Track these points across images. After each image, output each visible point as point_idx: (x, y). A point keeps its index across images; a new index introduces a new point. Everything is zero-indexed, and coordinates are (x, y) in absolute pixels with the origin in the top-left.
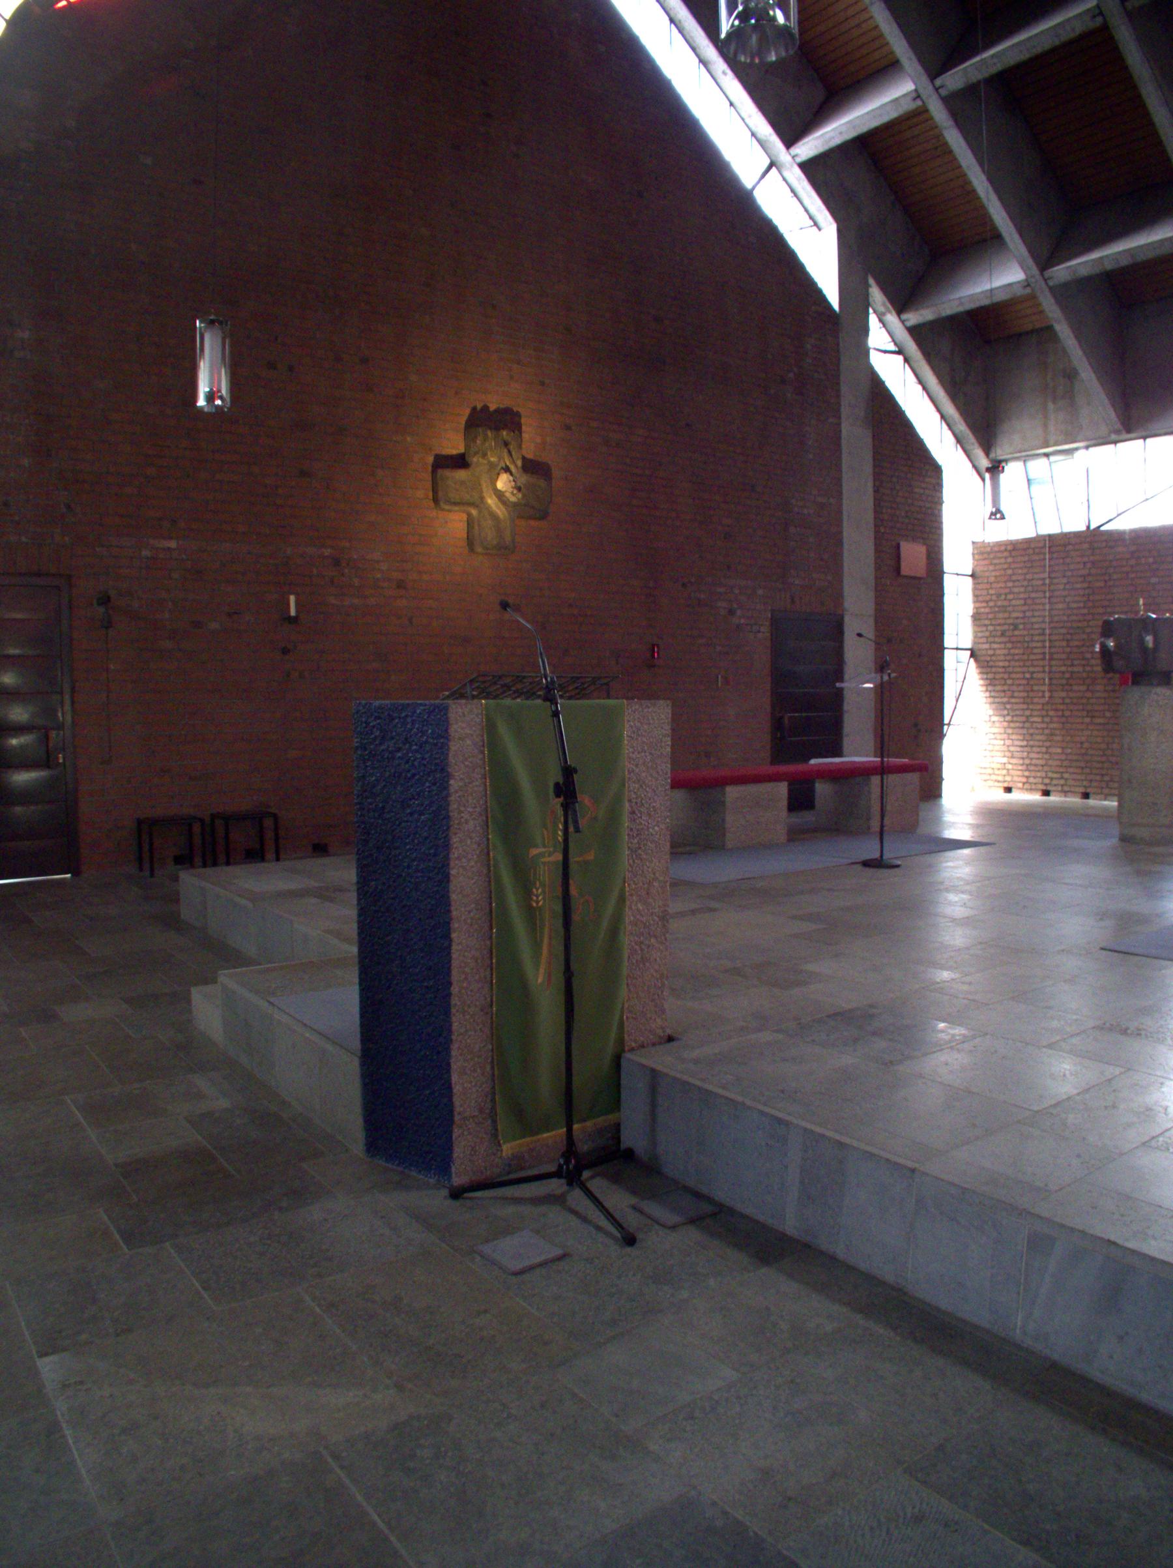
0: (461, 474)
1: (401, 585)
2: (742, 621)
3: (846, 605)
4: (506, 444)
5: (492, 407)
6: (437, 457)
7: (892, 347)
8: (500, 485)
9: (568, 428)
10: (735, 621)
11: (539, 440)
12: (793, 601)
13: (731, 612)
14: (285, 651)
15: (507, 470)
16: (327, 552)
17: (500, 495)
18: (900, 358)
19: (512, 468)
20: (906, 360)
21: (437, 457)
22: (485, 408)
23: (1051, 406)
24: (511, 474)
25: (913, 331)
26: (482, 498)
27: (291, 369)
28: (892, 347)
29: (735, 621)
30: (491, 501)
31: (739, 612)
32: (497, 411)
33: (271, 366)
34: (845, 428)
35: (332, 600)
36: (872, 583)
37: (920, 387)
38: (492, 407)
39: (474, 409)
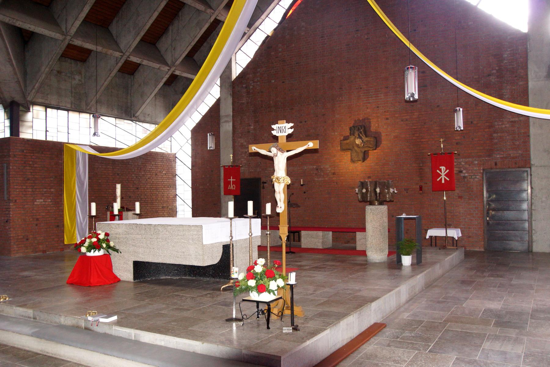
0: (348, 141)
1: (334, 174)
2: (466, 175)
3: (532, 162)
5: (361, 119)
6: (344, 137)
9: (387, 119)
10: (462, 175)
12: (496, 164)
13: (461, 172)
14: (305, 193)
15: (361, 138)
16: (315, 167)
17: (358, 146)
21: (344, 137)
22: (359, 120)
26: (353, 147)
27: (305, 122)
29: (462, 175)
30: (356, 148)
31: (464, 171)
32: (362, 120)
33: (301, 122)
34: (531, 84)
35: (316, 179)
38: (361, 119)
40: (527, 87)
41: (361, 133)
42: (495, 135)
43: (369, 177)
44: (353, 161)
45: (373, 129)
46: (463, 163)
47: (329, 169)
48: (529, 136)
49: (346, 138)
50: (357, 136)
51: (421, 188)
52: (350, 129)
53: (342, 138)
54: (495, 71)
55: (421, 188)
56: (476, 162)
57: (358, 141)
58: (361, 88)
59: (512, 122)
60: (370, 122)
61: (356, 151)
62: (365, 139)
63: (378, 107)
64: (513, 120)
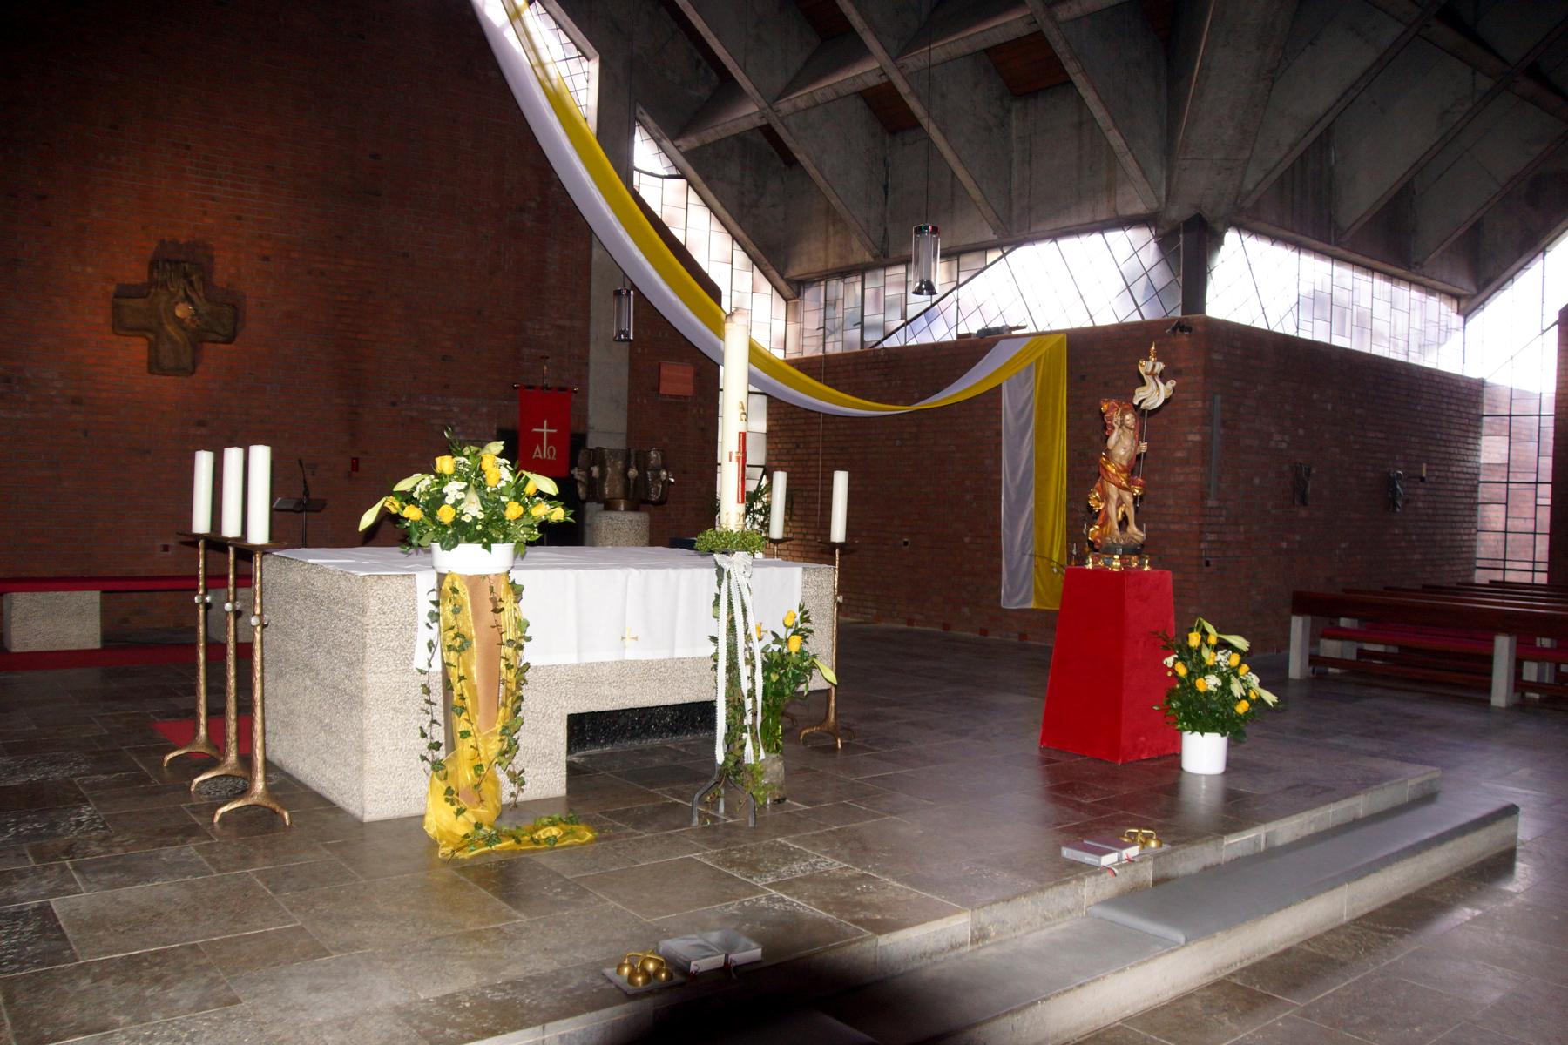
0: (139, 303)
1: (75, 401)
3: (592, 422)
4: (186, 275)
5: (182, 241)
7: (674, 172)
8: (178, 313)
9: (266, 259)
11: (233, 270)
18: (683, 183)
19: (194, 296)
20: (690, 184)
23: (831, 229)
24: (192, 302)
25: (686, 155)
26: (161, 324)
28: (674, 172)
36: (624, 401)
37: (707, 211)
38: (182, 241)
39: (162, 241)
40: (590, 256)
41: (191, 283)
42: (526, 351)
43: (201, 424)
44: (154, 366)
45: (221, 276)
46: (456, 409)
47: (58, 385)
48: (587, 364)
49: (124, 292)
50: (181, 293)
51: (355, 464)
52: (153, 265)
53: (112, 288)
54: (533, 204)
55: (355, 464)
56: (485, 410)
57: (182, 311)
58: (188, 147)
59: (559, 327)
60: (212, 258)
61: (170, 338)
62: (204, 308)
63: (239, 218)
64: (561, 322)
